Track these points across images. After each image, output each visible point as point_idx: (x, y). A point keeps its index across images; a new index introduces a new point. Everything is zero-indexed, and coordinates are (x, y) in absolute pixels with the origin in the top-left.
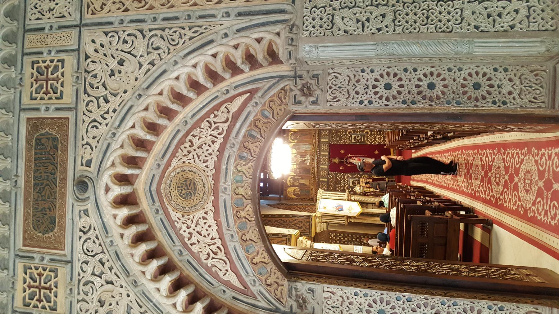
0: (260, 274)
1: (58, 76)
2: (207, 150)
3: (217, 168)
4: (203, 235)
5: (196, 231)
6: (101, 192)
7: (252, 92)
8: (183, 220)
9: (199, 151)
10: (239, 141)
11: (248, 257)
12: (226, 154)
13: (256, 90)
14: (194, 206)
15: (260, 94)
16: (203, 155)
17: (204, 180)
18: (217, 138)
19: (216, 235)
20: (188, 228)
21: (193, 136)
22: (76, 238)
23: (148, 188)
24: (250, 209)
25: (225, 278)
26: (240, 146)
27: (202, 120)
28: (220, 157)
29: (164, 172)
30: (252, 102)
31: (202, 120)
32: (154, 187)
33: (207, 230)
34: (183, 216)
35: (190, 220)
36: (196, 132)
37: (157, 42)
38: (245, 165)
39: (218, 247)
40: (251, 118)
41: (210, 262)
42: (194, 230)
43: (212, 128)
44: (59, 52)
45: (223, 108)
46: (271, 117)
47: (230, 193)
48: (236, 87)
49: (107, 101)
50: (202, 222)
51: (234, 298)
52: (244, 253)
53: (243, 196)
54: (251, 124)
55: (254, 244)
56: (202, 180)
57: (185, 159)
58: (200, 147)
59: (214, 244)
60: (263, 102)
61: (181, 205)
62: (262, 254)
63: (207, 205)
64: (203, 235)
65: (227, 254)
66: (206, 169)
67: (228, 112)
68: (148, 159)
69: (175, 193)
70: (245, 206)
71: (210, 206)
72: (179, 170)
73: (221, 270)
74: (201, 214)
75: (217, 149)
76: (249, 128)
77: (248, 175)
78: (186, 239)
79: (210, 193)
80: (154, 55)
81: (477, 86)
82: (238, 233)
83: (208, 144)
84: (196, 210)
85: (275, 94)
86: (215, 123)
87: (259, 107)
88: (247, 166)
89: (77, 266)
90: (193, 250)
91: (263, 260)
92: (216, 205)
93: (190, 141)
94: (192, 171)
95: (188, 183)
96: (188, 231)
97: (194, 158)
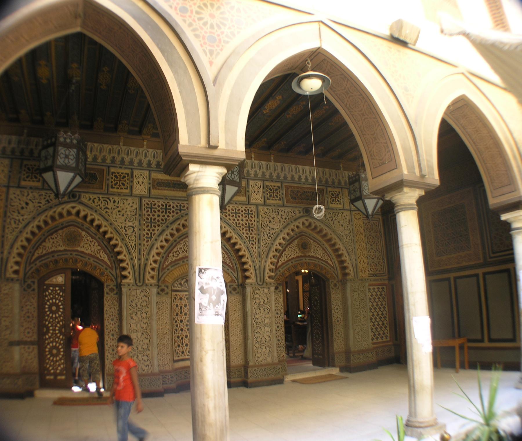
6: (306, 218)
7: (333, 268)
22: (292, 208)
28: (315, 257)
32: (304, 234)
36: (321, 249)
37: (348, 238)
41: (283, 255)
44: (343, 202)
49: (332, 220)
65: (287, 261)
71: (300, 254)
74: (298, 251)
80: (345, 237)
81: (339, 333)
89: (283, 209)
92: (301, 256)
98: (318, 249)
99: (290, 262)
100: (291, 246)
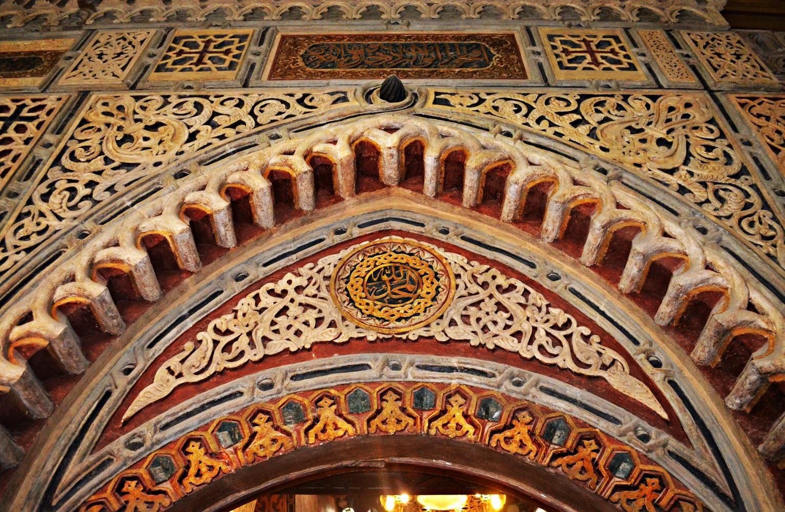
0: (155, 463)
1: (602, 63)
2: (495, 323)
3: (451, 346)
4: (277, 320)
5: (289, 304)
7: (672, 425)
8: (319, 278)
9: (489, 306)
10: (529, 398)
11: (205, 428)
12: (488, 366)
13: (682, 437)
14: (351, 301)
15: (674, 444)
16: (481, 314)
17: (416, 319)
18: (531, 342)
19: (275, 347)
20: (299, 289)
21: (526, 293)
23: (394, 214)
24: (340, 433)
25: (161, 372)
26: (516, 400)
27: (568, 308)
28: (480, 351)
29: (431, 240)
30: (645, 427)
31: (568, 308)
32: (397, 225)
33: (289, 327)
34: (326, 278)
35: (314, 292)
36: (536, 297)
38: (466, 416)
39: (242, 354)
40: (603, 425)
41: (207, 336)
42: (292, 301)
43: (555, 333)
45: (610, 354)
46: (616, 481)
47: (384, 378)
48: (673, 384)
50: (311, 315)
51: (108, 394)
52: (217, 418)
53: (379, 412)
54: (584, 425)
55: (240, 445)
56: (417, 314)
57: (465, 277)
58: (500, 307)
59: (252, 344)
60: (652, 456)
61: (354, 274)
62: (211, 468)
63: (352, 326)
64: (277, 320)
65: (223, 375)
66: (446, 322)
67: (604, 367)
68: (457, 209)
69: (383, 261)
70: (350, 417)
71: (348, 333)
72: (437, 267)
73: (182, 362)
74: (330, 311)
75: (502, 344)
76: (570, 421)
77: (438, 423)
78: (270, 286)
79: (384, 331)
82: (274, 401)
83: (509, 323)
84: (339, 306)
85: (686, 488)
86: (569, 337)
87: (638, 447)
88: (462, 421)
90: (243, 301)
91: (193, 471)
93: (512, 287)
94: (438, 292)
95: (409, 287)
96: (291, 289)
97: (470, 294)
98: (511, 301)
99: (243, 383)
100: (281, 285)
